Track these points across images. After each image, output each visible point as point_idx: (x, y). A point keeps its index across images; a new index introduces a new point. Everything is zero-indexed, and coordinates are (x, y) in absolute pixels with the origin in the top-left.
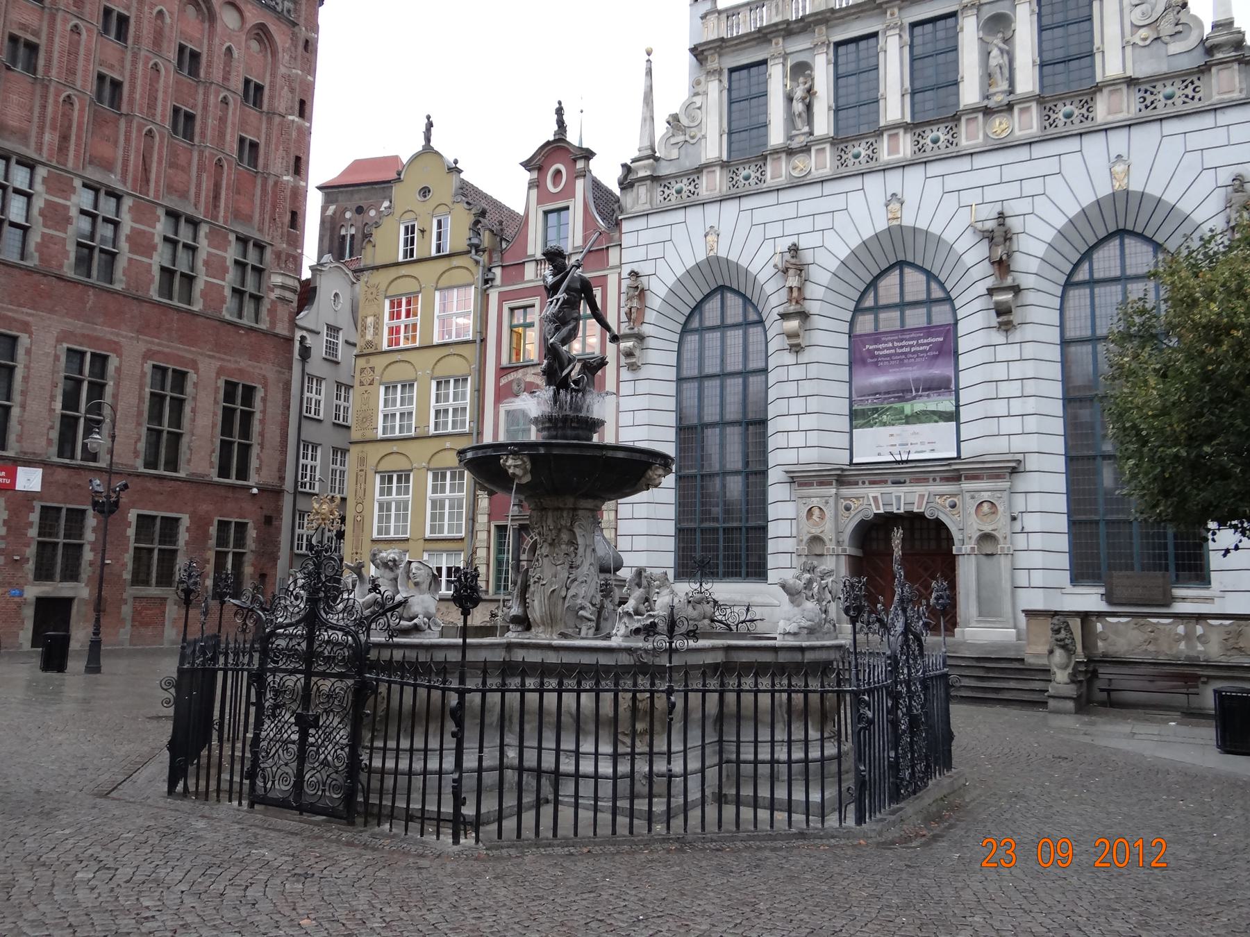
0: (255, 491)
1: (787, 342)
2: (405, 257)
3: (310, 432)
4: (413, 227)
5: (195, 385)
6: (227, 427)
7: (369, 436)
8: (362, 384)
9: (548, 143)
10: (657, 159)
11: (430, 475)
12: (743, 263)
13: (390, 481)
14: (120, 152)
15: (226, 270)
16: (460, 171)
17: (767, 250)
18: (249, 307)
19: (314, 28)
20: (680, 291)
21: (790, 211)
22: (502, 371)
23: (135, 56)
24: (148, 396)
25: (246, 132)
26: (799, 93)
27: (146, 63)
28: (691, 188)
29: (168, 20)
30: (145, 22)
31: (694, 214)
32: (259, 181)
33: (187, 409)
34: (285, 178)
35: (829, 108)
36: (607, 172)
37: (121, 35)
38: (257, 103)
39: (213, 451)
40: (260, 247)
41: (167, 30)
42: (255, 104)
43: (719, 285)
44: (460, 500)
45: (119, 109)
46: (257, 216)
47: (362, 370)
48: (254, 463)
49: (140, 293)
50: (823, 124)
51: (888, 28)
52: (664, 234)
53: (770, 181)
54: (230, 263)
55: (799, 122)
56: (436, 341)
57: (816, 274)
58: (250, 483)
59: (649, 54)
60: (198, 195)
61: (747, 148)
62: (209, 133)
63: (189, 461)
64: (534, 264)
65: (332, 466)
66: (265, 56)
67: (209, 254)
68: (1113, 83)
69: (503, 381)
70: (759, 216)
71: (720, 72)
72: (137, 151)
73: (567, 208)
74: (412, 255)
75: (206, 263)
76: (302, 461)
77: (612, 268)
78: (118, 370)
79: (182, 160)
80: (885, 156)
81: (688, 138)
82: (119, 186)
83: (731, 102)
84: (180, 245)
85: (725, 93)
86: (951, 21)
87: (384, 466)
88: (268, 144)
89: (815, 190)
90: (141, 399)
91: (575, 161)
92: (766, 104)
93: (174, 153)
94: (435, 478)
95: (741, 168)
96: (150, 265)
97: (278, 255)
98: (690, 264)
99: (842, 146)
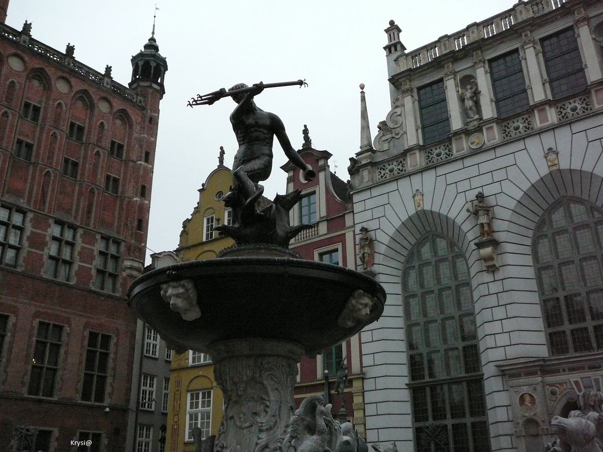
0: (107, 410)
1: (484, 265)
2: (207, 238)
3: (148, 366)
4: (212, 218)
5: (68, 334)
7: (183, 364)
10: (374, 152)
12: (444, 212)
13: (197, 398)
14: (28, 185)
15: (93, 258)
17: (460, 201)
18: (109, 283)
19: (158, 111)
20: (399, 238)
21: (474, 171)
23: (42, 128)
24: (34, 343)
25: (111, 173)
26: (468, 94)
27: (48, 133)
29: (64, 108)
30: (50, 109)
31: (404, 183)
32: (118, 202)
33: (62, 351)
34: (135, 199)
35: (492, 101)
36: (340, 167)
37: (35, 119)
38: (119, 155)
40: (117, 243)
41: (63, 114)
42: (118, 156)
43: (427, 228)
45: (30, 160)
46: (116, 224)
48: (108, 389)
49: (34, 274)
50: (488, 111)
51: (525, 43)
52: (383, 200)
54: (96, 253)
55: (471, 114)
57: (498, 212)
58: (105, 404)
59: (362, 87)
60: (77, 211)
61: (437, 137)
62: (86, 174)
63: (61, 389)
65: (164, 391)
66: (125, 128)
67: (82, 248)
70: (451, 178)
71: (411, 90)
72: (39, 184)
73: (314, 193)
74: (211, 237)
75: (80, 254)
76: (142, 388)
77: (349, 228)
80: (538, 124)
81: (394, 135)
82: (25, 206)
83: (421, 108)
84: (64, 242)
85: (417, 103)
86: (569, 34)
87: (194, 386)
88: (124, 179)
90: (29, 346)
91: (317, 161)
92: (446, 106)
95: (434, 149)
96: (42, 255)
97: (129, 248)
98: (404, 217)
99: (505, 123)
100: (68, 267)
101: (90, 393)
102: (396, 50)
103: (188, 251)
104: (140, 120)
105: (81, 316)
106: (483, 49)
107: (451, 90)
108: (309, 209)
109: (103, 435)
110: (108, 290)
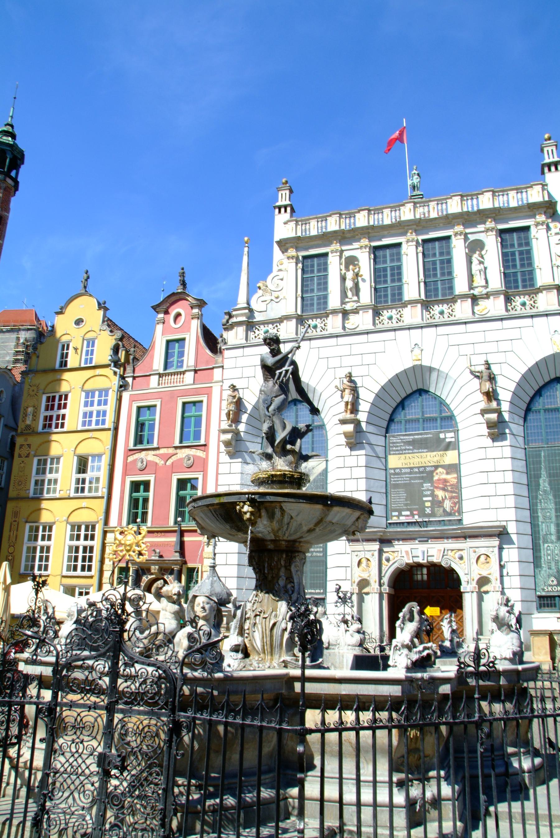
4: (68, 346)
7: (23, 494)
11: (69, 527)
21: (345, 350)
26: (350, 275)
50: (366, 296)
53: (330, 330)
55: (349, 294)
57: (362, 393)
64: (157, 377)
68: (548, 288)
69: (130, 459)
70: (324, 353)
81: (274, 299)
89: (364, 338)
91: (192, 308)
102: (286, 211)
106: (370, 235)
107: (334, 265)
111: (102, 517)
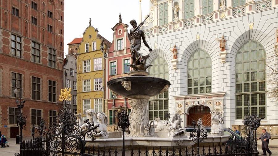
0: (57, 104)
4: (88, 44)
5: (42, 81)
6: (50, 90)
7: (81, 92)
8: (79, 80)
9: (118, 23)
11: (94, 99)
13: (86, 101)
16: (98, 31)
22: (109, 76)
28: (151, 33)
33: (41, 86)
39: (47, 96)
44: (101, 105)
47: (79, 77)
54: (48, 54)
56: (94, 70)
58: (56, 102)
60: (39, 38)
62: (41, 24)
66: (52, 6)
67: (43, 52)
73: (122, 39)
74: (88, 51)
75: (42, 54)
78: (24, 77)
79: (35, 29)
91: (124, 27)
93: (33, 28)
94: (96, 100)
100: (38, 58)
101: (51, 99)
103: (80, 55)
104: (57, 3)
105: (46, 75)
108: (121, 44)
109: (57, 111)
110: (53, 67)
111: (103, 96)
